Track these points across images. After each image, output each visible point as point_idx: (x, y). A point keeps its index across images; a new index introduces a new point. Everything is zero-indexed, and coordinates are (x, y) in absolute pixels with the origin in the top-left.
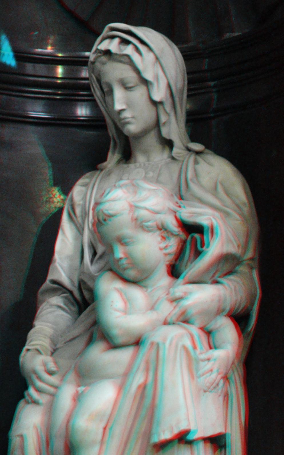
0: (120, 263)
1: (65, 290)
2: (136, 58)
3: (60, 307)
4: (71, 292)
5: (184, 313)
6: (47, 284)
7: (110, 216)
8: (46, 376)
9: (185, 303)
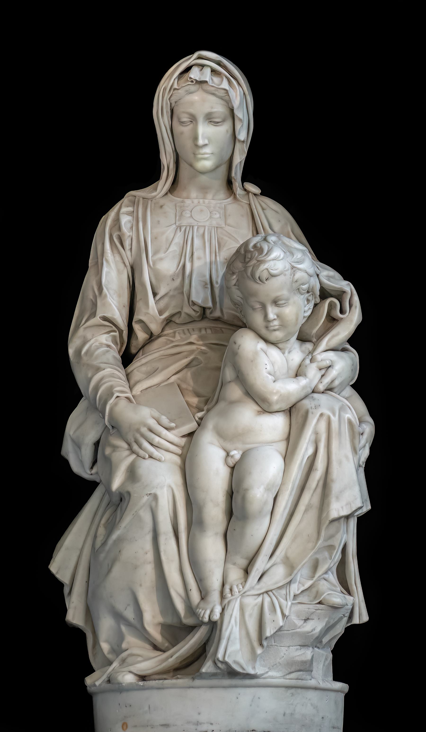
0: (271, 324)
1: (114, 328)
2: (232, 93)
3: (108, 346)
4: (121, 332)
5: (332, 381)
6: (97, 320)
7: (273, 276)
8: (164, 432)
9: (333, 373)
